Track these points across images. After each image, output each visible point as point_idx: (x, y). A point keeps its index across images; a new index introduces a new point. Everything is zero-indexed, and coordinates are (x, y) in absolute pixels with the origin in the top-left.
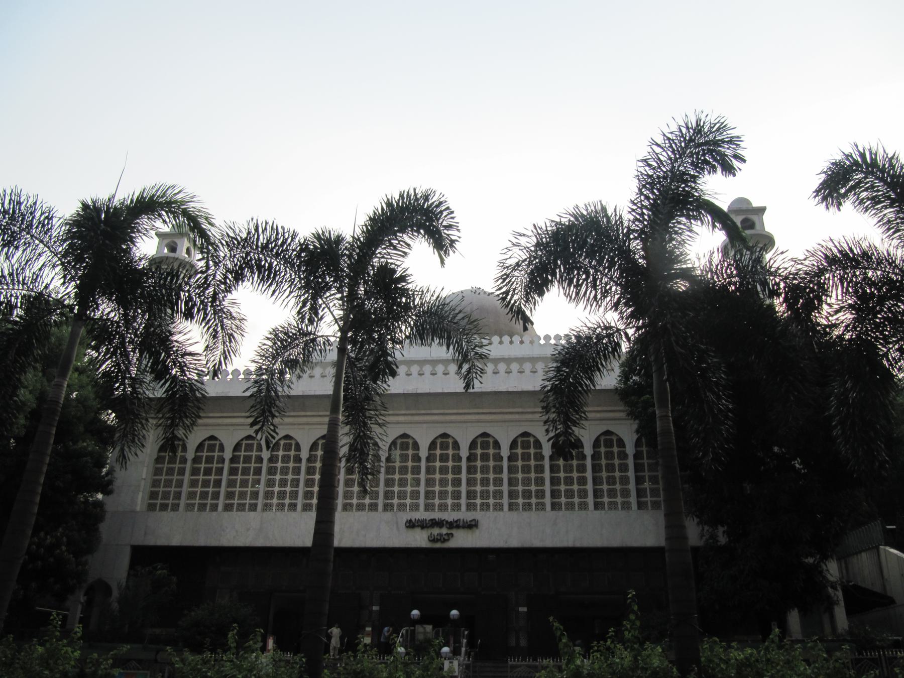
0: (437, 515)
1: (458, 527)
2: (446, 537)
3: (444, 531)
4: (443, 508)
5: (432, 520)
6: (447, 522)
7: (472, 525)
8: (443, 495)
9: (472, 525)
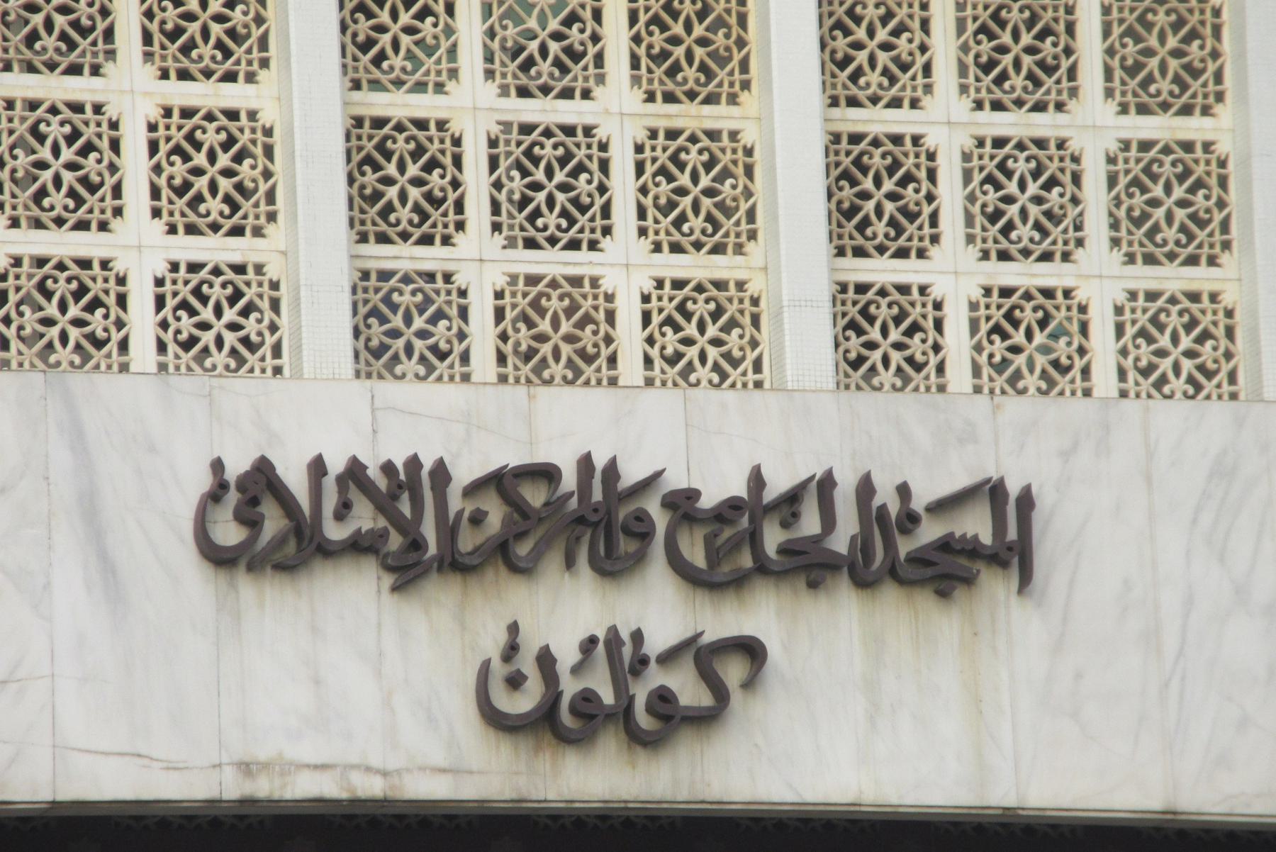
0: (566, 427)
1: (809, 567)
2: (687, 688)
3: (659, 610)
4: (556, 338)
5: (500, 482)
6: (683, 505)
7: (958, 553)
8: (552, 189)
9: (958, 553)
